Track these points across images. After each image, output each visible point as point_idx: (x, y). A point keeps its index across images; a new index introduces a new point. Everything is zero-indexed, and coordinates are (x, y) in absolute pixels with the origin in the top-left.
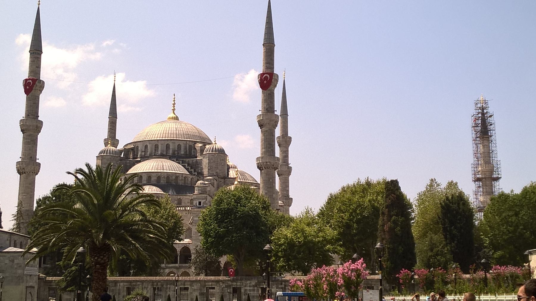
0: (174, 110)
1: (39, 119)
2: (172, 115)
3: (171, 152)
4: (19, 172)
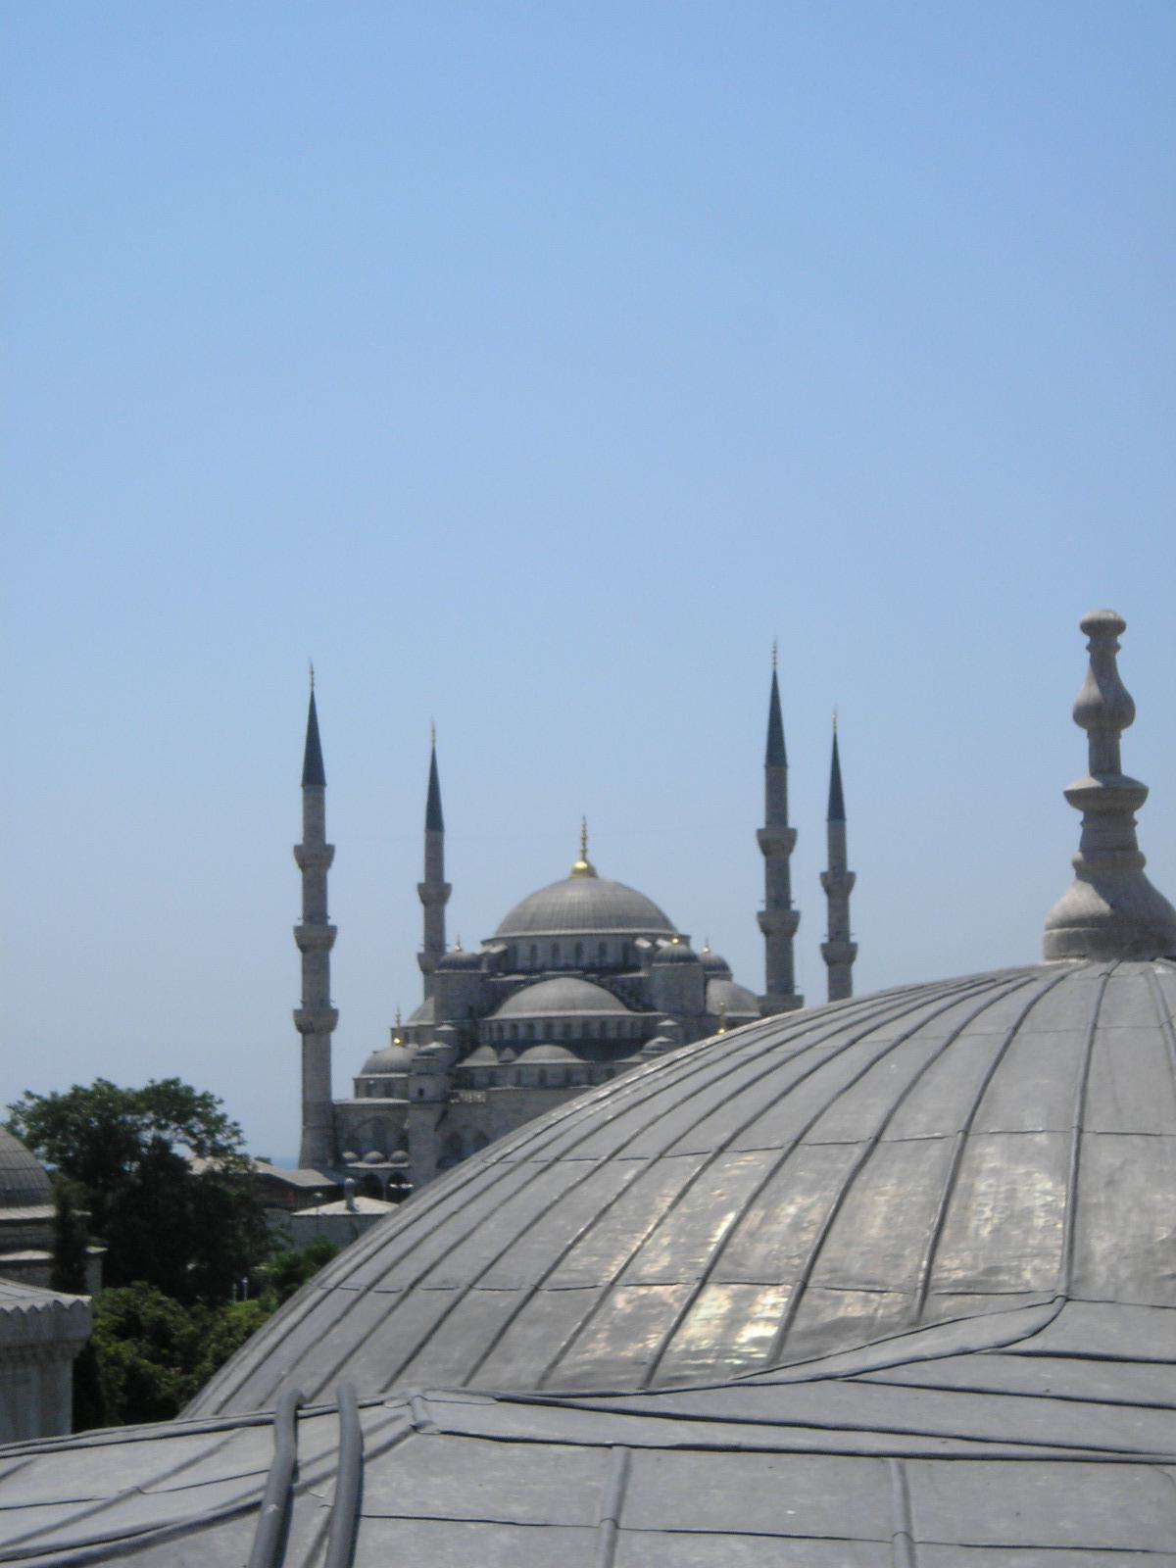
0: (584, 851)
2: (581, 865)
4: (300, 1028)
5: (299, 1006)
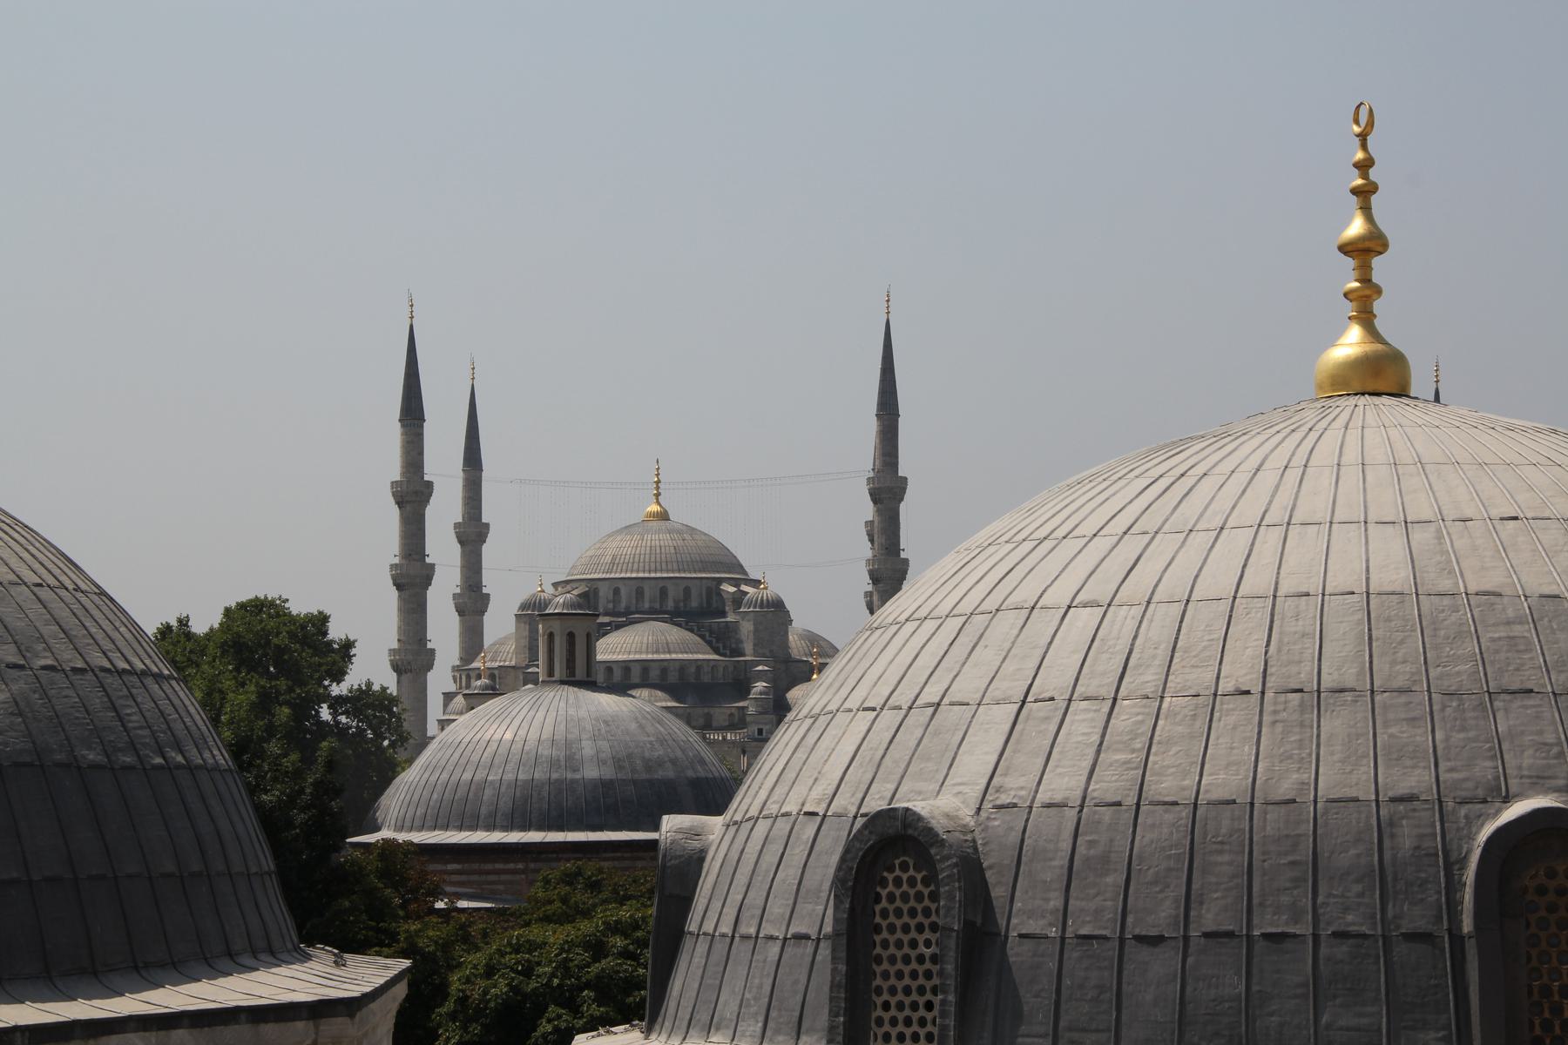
0: (658, 495)
1: (428, 560)
2: (655, 508)
3: (670, 605)
5: (395, 645)
